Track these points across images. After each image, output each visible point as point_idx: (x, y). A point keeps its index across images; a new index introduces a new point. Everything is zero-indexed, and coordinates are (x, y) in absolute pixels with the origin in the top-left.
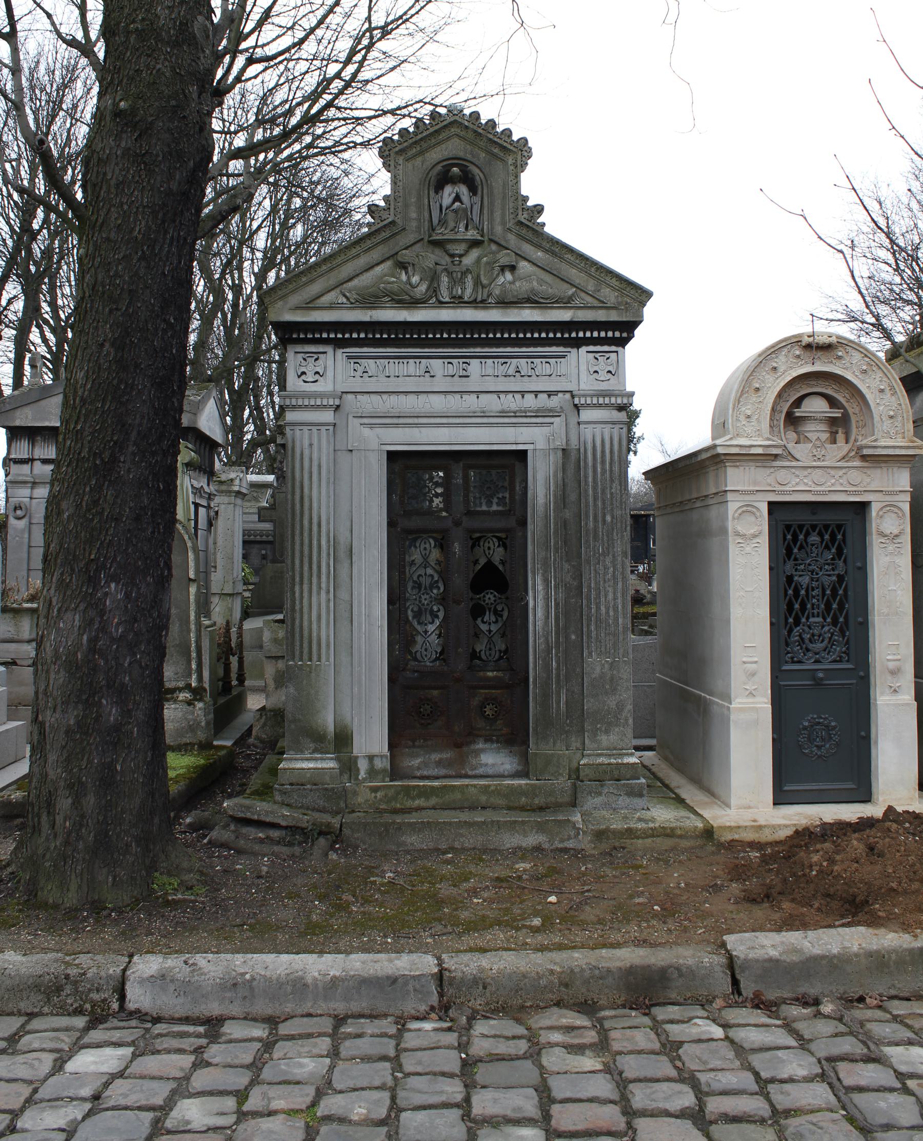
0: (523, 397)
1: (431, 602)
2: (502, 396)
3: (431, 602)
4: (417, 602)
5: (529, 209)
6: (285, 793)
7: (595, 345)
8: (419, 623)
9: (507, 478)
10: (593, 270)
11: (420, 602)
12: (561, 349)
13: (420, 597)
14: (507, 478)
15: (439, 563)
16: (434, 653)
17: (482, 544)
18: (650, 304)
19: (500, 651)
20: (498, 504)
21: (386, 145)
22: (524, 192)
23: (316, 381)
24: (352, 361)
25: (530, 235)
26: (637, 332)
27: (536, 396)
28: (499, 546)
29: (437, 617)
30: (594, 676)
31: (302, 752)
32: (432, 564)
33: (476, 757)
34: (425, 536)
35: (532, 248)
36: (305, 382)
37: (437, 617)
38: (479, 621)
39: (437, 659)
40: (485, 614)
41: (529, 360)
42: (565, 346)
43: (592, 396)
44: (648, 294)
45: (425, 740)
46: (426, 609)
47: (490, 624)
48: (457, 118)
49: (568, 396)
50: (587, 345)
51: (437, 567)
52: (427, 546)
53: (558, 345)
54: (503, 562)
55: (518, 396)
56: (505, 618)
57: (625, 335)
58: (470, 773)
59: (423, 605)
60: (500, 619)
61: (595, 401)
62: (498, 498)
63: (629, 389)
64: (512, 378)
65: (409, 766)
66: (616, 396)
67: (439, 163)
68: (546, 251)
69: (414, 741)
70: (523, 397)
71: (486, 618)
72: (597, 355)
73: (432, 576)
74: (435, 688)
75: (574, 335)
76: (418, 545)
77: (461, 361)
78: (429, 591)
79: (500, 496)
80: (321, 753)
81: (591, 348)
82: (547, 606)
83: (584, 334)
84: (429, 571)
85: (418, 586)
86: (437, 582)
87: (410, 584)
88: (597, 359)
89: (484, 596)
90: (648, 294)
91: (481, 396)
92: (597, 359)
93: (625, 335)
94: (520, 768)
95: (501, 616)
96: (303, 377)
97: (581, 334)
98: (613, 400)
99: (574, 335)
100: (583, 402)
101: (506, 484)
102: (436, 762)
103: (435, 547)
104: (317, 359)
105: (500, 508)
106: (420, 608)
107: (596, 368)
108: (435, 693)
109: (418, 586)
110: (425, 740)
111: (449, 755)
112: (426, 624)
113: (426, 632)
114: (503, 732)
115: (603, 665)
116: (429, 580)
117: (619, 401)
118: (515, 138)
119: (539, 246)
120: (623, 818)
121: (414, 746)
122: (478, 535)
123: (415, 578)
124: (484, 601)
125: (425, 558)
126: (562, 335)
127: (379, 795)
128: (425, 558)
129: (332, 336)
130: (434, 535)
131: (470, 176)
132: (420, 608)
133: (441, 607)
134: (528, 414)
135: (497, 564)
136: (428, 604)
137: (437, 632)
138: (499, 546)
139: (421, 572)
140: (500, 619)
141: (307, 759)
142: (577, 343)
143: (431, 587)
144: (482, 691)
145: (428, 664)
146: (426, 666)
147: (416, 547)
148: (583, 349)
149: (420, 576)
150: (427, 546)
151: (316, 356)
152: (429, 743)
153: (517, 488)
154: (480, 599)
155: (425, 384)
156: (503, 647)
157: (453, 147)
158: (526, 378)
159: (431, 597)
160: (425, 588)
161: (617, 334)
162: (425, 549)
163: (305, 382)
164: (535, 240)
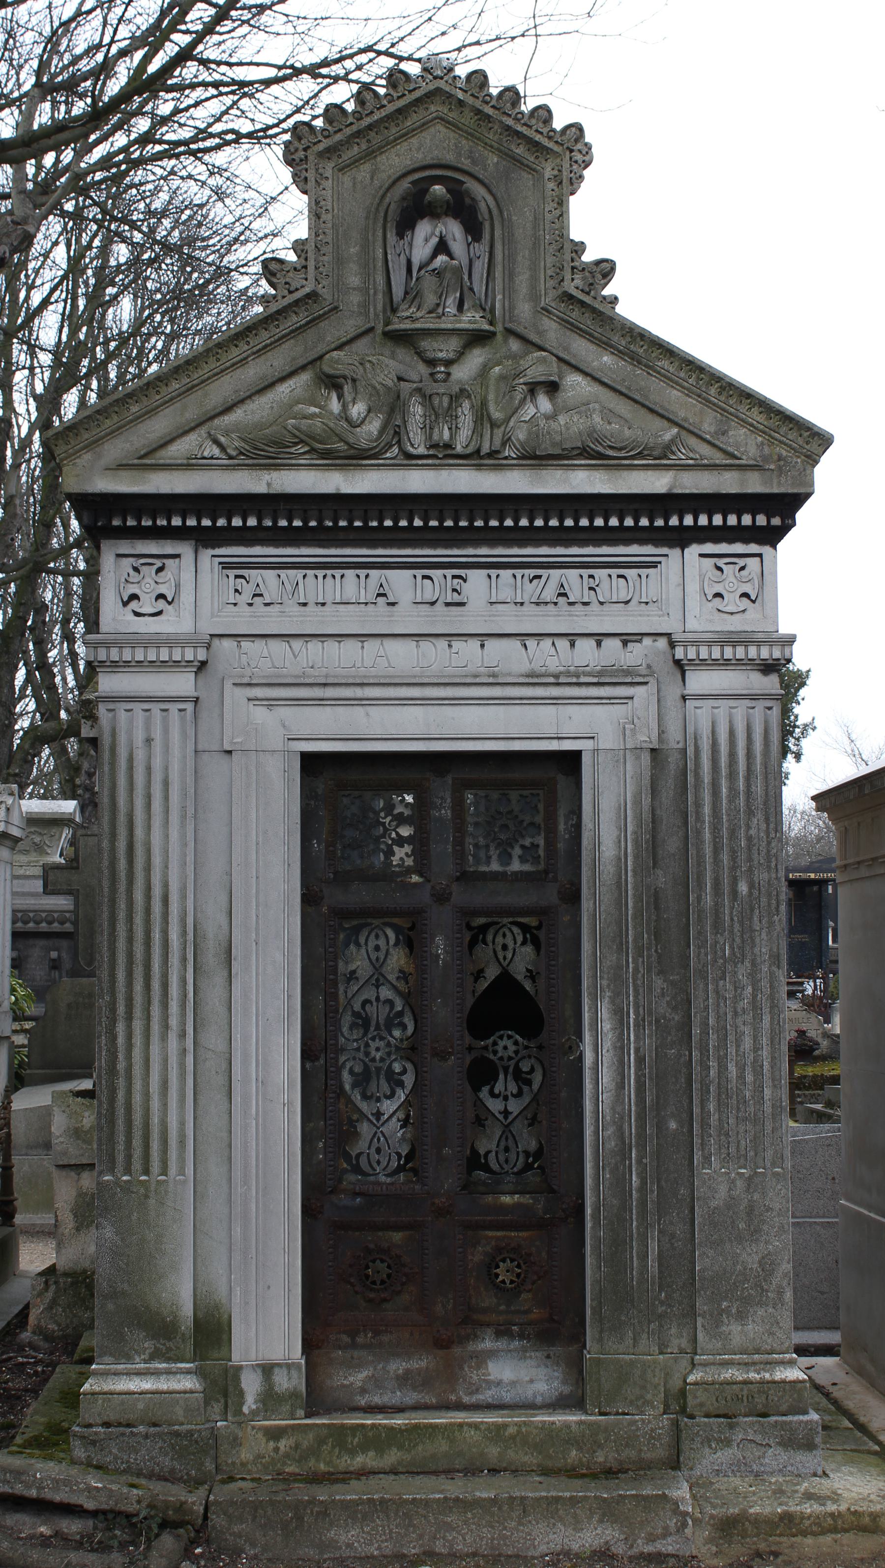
0: (573, 645)
1: (389, 1054)
2: (531, 643)
3: (389, 1054)
4: (361, 1055)
5: (585, 268)
7: (716, 541)
8: (365, 1097)
9: (541, 807)
10: (713, 391)
11: (367, 1054)
12: (649, 549)
13: (367, 1045)
14: (541, 807)
15: (404, 976)
16: (395, 1157)
17: (490, 938)
18: (827, 459)
19: (527, 1154)
20: (522, 859)
21: (300, 139)
22: (575, 234)
23: (159, 613)
24: (232, 573)
25: (587, 321)
26: (801, 515)
27: (599, 644)
28: (524, 943)
29: (401, 1084)
30: (713, 1204)
31: (129, 1359)
32: (392, 977)
33: (478, 1367)
34: (376, 922)
36: (137, 614)
37: (401, 1084)
38: (484, 1093)
39: (400, 1169)
40: (496, 1079)
41: (585, 572)
42: (657, 543)
43: (710, 644)
44: (823, 440)
45: (376, 1333)
46: (378, 1070)
47: (506, 1098)
48: (441, 84)
49: (662, 643)
50: (701, 541)
51: (401, 985)
52: (382, 942)
53: (642, 542)
54: (532, 975)
56: (536, 1086)
57: (776, 521)
58: (466, 1399)
59: (373, 1060)
60: (525, 1088)
61: (716, 654)
62: (523, 847)
63: (784, 628)
64: (551, 607)
65: (343, 1386)
66: (759, 644)
67: (404, 175)
68: (620, 353)
69: (353, 1334)
70: (573, 645)
71: (499, 1087)
72: (721, 562)
73: (390, 1003)
74: (397, 1228)
75: (674, 521)
76: (362, 940)
77: (449, 573)
78: (384, 1034)
79: (527, 842)
80: (168, 1360)
81: (709, 548)
82: (621, 1063)
83: (696, 520)
84: (386, 993)
85: (363, 1022)
86: (400, 1014)
87: (347, 1020)
88: (719, 569)
89: (495, 1044)
90: (823, 440)
91: (490, 643)
92: (719, 569)
93: (776, 521)
94: (567, 1390)
95: (529, 1083)
96: (134, 605)
97: (688, 520)
98: (753, 652)
99: (674, 521)
100: (692, 655)
101: (539, 819)
102: (398, 1377)
103: (396, 944)
104: (160, 570)
105: (527, 867)
106: (366, 1066)
107: (718, 588)
108: (397, 1237)
109: (363, 1022)
110: (376, 1333)
111: (423, 1364)
112: (378, 1100)
113: (378, 1114)
114: (532, 1316)
115: (734, 1182)
116: (385, 1011)
117: (765, 653)
118: (558, 124)
119: (605, 344)
120: (774, 1492)
121: (354, 1345)
122: (482, 921)
123: (357, 1007)
124: (495, 1052)
125: (377, 966)
126: (651, 522)
127: (283, 1444)
128: (377, 966)
129: (191, 522)
130: (396, 920)
131: (468, 201)
132: (366, 1066)
133: (409, 1066)
134: (583, 679)
135: (520, 978)
136: (382, 1060)
137: (401, 1115)
138: (524, 943)
139: (369, 993)
140: (525, 1088)
141: (139, 1373)
142: (681, 538)
143: (389, 1025)
144: (490, 1233)
145: (382, 1179)
146: (379, 1184)
147: (358, 945)
148: (694, 550)
149: (366, 1002)
150: (382, 942)
151: (158, 563)
152: (385, 1338)
153: (562, 827)
154: (486, 1048)
155: (377, 619)
156: (533, 1146)
157: (432, 144)
158: (579, 607)
159: (389, 1044)
160: (378, 1027)
161: (761, 520)
162: (377, 948)
163: (137, 614)
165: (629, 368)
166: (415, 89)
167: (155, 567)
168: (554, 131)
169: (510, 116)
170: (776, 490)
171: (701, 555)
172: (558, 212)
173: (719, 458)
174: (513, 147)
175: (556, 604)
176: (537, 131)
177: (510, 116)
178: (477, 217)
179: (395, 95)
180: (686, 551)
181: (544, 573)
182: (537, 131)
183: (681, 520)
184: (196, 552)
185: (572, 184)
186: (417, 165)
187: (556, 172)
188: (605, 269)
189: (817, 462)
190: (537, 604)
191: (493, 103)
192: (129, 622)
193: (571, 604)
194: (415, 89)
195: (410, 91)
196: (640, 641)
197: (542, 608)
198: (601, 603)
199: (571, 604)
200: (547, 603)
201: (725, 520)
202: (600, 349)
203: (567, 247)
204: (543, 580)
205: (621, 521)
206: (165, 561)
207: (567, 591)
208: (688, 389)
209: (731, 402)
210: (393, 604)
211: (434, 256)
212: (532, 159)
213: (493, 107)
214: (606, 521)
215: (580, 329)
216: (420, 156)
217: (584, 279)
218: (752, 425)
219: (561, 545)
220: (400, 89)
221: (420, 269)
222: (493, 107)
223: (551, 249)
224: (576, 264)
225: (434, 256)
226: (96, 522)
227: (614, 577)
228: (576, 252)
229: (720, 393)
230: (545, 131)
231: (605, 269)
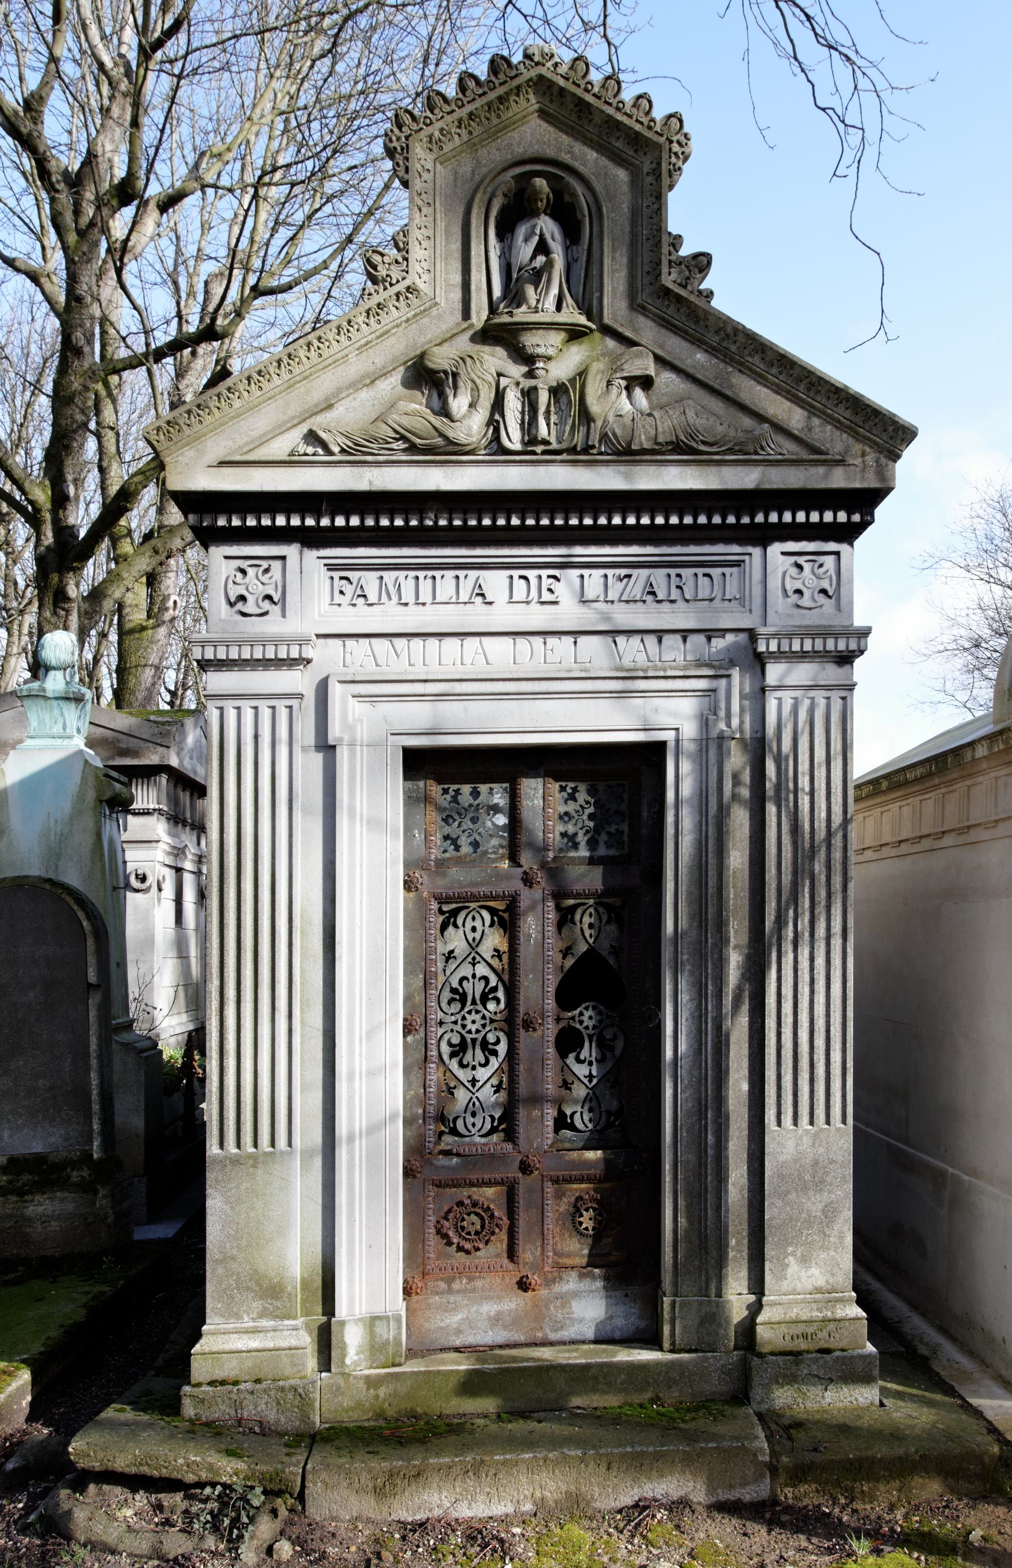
0: (660, 641)
1: (484, 1026)
2: (621, 640)
3: (484, 1026)
4: (458, 1028)
5: (680, 262)
6: (203, 1401)
7: (797, 539)
8: (462, 1065)
9: (626, 796)
10: (802, 387)
11: (464, 1026)
12: (736, 549)
13: (464, 1018)
14: (626, 796)
15: (498, 954)
16: (488, 1120)
17: (577, 917)
18: (910, 454)
19: (609, 1113)
20: (608, 845)
21: (400, 126)
22: (673, 226)
23: (266, 613)
24: (336, 575)
25: (680, 319)
26: (880, 511)
27: (685, 640)
28: (608, 922)
29: (495, 1053)
30: (782, 1158)
31: (238, 1317)
32: (487, 956)
33: (563, 1306)
34: (473, 905)
35: (685, 344)
36: (244, 615)
37: (495, 1053)
38: (571, 1060)
39: (493, 1130)
40: (582, 1047)
41: (673, 572)
42: (741, 541)
43: (790, 636)
44: (905, 434)
45: (471, 1279)
46: (474, 1041)
47: (590, 1064)
48: (543, 71)
49: (743, 637)
50: (783, 539)
51: (495, 963)
52: (478, 924)
53: (727, 541)
54: (615, 951)
55: (651, 640)
56: (618, 1052)
57: (856, 518)
58: (553, 1336)
59: (470, 1032)
60: (609, 1055)
61: (796, 647)
62: (609, 833)
63: (859, 621)
64: (640, 604)
66: (836, 636)
67: (505, 170)
68: (712, 351)
70: (660, 641)
71: (584, 1054)
72: (801, 560)
73: (486, 979)
74: (488, 1184)
75: (760, 518)
76: (460, 922)
77: (545, 573)
78: (480, 1007)
79: (613, 829)
80: (276, 1317)
81: (791, 546)
82: (699, 1031)
83: (780, 517)
84: (482, 970)
85: (460, 996)
86: (495, 989)
87: (447, 995)
88: (800, 567)
89: (581, 1014)
90: (905, 434)
91: (582, 640)
92: (800, 567)
93: (856, 518)
94: (642, 1324)
95: (612, 1049)
96: (240, 606)
97: (774, 518)
98: (830, 644)
99: (760, 518)
100: (773, 647)
101: (624, 807)
102: (490, 1318)
103: (492, 925)
104: (267, 571)
105: (612, 852)
106: (463, 1037)
107: (798, 585)
108: (490, 1192)
109: (460, 996)
110: (471, 1279)
111: (513, 1306)
112: (474, 1068)
113: (474, 1081)
114: (612, 1258)
115: (801, 1138)
116: (480, 986)
117: (842, 646)
118: (659, 113)
119: (697, 341)
122: (571, 902)
123: (455, 984)
124: (581, 1022)
125: (474, 946)
126: (738, 519)
128: (474, 946)
129: (296, 521)
130: (491, 904)
131: (567, 198)
132: (463, 1037)
133: (501, 1035)
134: (669, 673)
135: (604, 953)
136: (478, 1031)
137: (495, 1081)
138: (608, 922)
139: (466, 970)
140: (609, 1055)
142: (764, 536)
143: (484, 998)
144: (575, 1186)
145: (477, 1139)
146: (475, 1144)
147: (456, 926)
148: (775, 549)
149: (464, 979)
150: (478, 924)
151: (265, 564)
152: (479, 1284)
153: (645, 814)
154: (573, 1018)
155: (476, 617)
156: (614, 1105)
157: (532, 133)
158: (666, 605)
159: (484, 1017)
160: (474, 1002)
161: (842, 517)
162: (474, 929)
163: (244, 615)
164: (690, 326)
165: (722, 365)
166: (516, 76)
167: (262, 569)
168: (653, 120)
169: (610, 104)
170: (857, 485)
171: (783, 553)
172: (656, 206)
173: (805, 455)
174: (613, 140)
175: (644, 601)
176: (637, 121)
177: (610, 104)
178: (575, 216)
179: (497, 82)
180: (769, 549)
181: (635, 572)
182: (637, 121)
183: (766, 517)
184: (301, 553)
185: (670, 176)
186: (517, 159)
187: (654, 166)
188: (702, 262)
189: (899, 457)
190: (627, 602)
191: (596, 90)
192: (236, 622)
193: (659, 602)
194: (516, 76)
195: (512, 78)
196: (723, 637)
197: (632, 605)
198: (687, 601)
199: (659, 602)
200: (635, 601)
201: (808, 517)
202: (693, 347)
203: (665, 240)
204: (633, 579)
205: (710, 519)
206: (271, 562)
207: (656, 589)
208: (777, 385)
209: (818, 398)
210: (491, 603)
211: (533, 257)
212: (631, 153)
213: (594, 95)
214: (695, 519)
215: (675, 326)
216: (521, 151)
217: (680, 273)
218: (839, 421)
219: (651, 544)
220: (501, 76)
221: (520, 270)
222: (594, 95)
223: (647, 245)
224: (673, 258)
225: (533, 257)
226: (201, 522)
227: (700, 576)
228: (673, 245)
229: (809, 389)
230: (645, 120)
231: (702, 262)
